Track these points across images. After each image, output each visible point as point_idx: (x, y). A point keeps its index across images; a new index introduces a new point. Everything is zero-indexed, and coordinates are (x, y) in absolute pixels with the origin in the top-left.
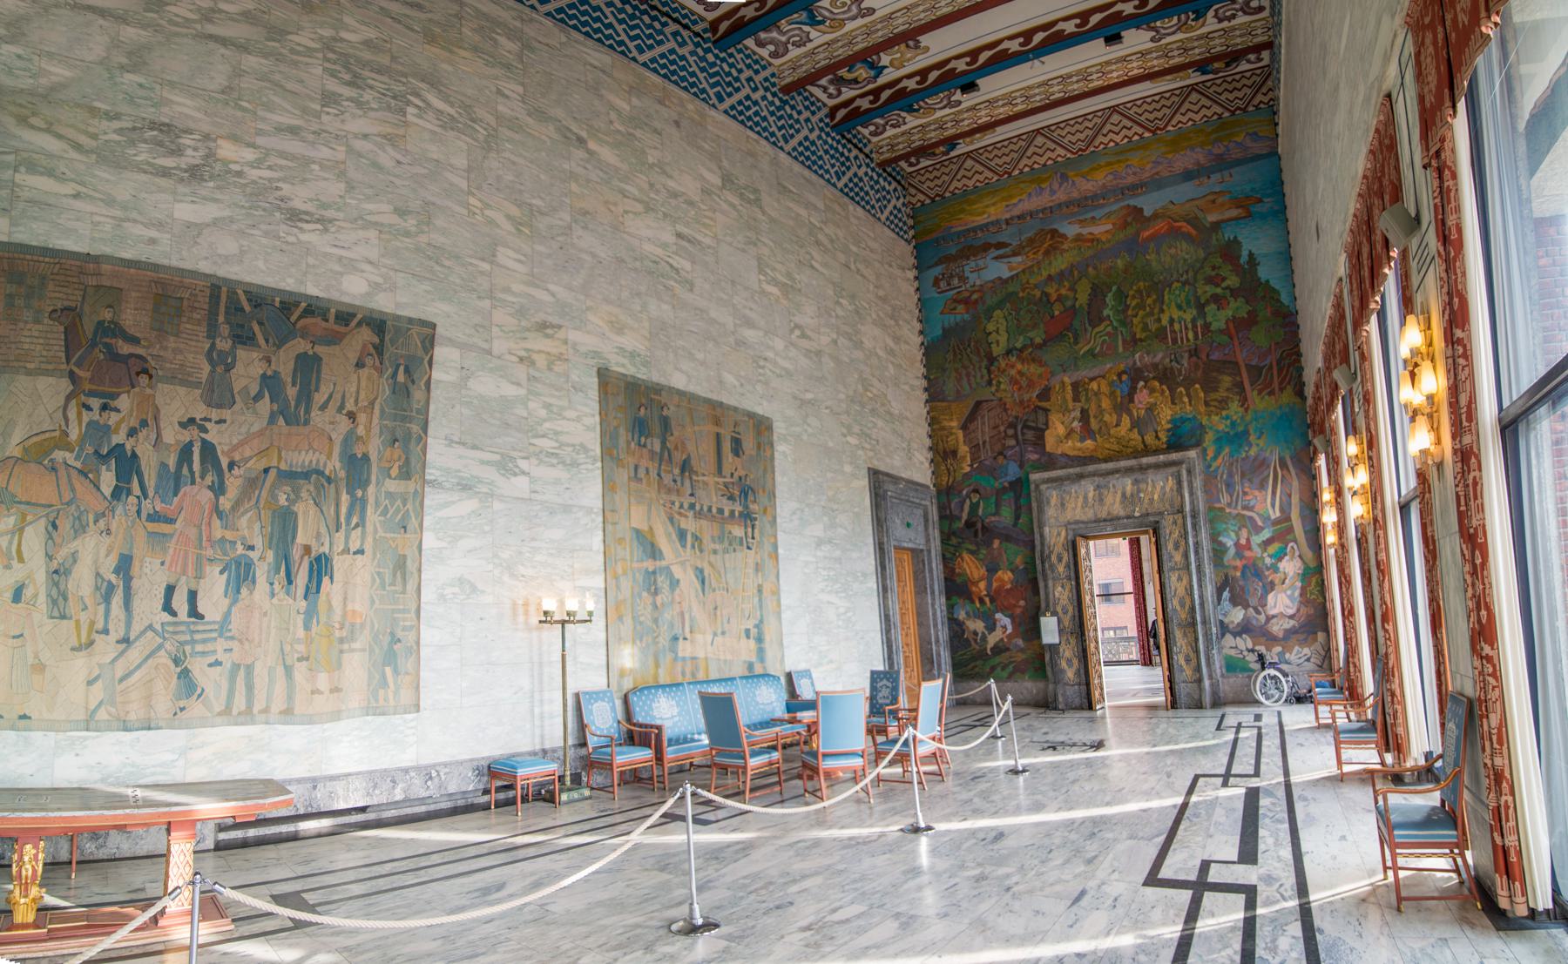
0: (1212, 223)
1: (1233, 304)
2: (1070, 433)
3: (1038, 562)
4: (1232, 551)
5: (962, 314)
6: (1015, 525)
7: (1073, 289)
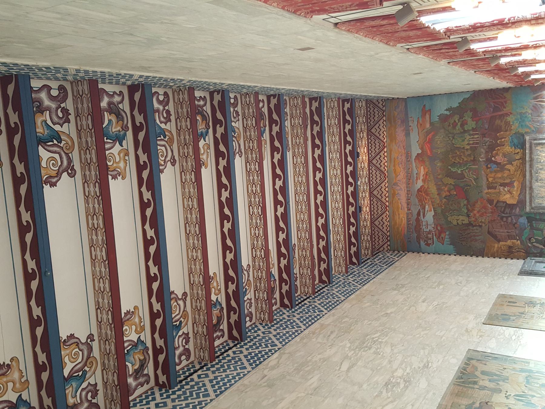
0: (430, 125)
1: (466, 118)
5: (446, 236)
7: (446, 185)
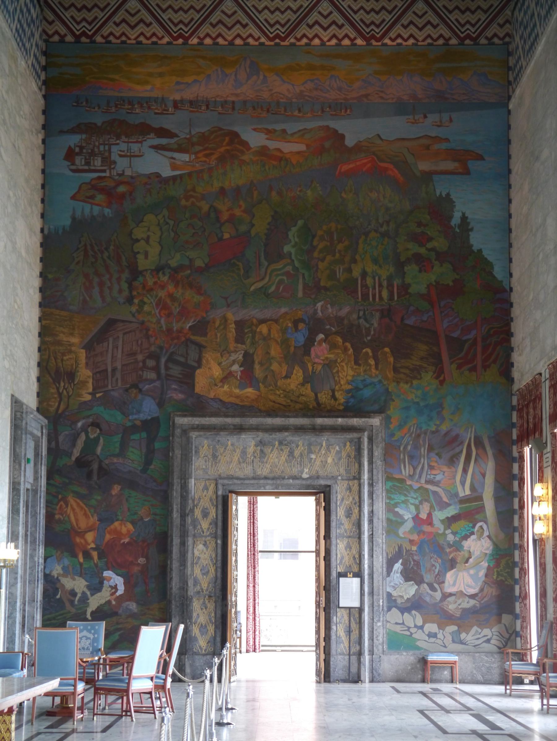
0: (424, 173)
2: (227, 377)
3: (176, 515)
4: (409, 524)
6: (144, 471)
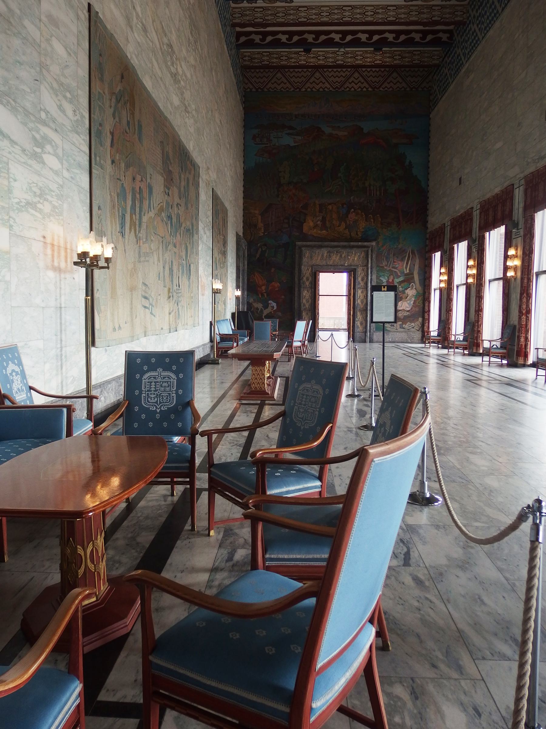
2: (316, 226)
3: (296, 279)
